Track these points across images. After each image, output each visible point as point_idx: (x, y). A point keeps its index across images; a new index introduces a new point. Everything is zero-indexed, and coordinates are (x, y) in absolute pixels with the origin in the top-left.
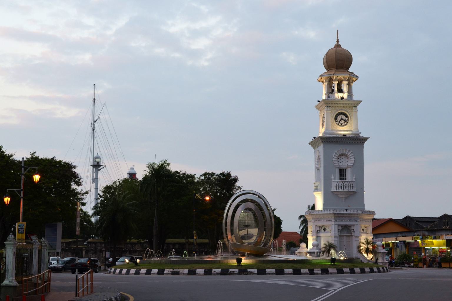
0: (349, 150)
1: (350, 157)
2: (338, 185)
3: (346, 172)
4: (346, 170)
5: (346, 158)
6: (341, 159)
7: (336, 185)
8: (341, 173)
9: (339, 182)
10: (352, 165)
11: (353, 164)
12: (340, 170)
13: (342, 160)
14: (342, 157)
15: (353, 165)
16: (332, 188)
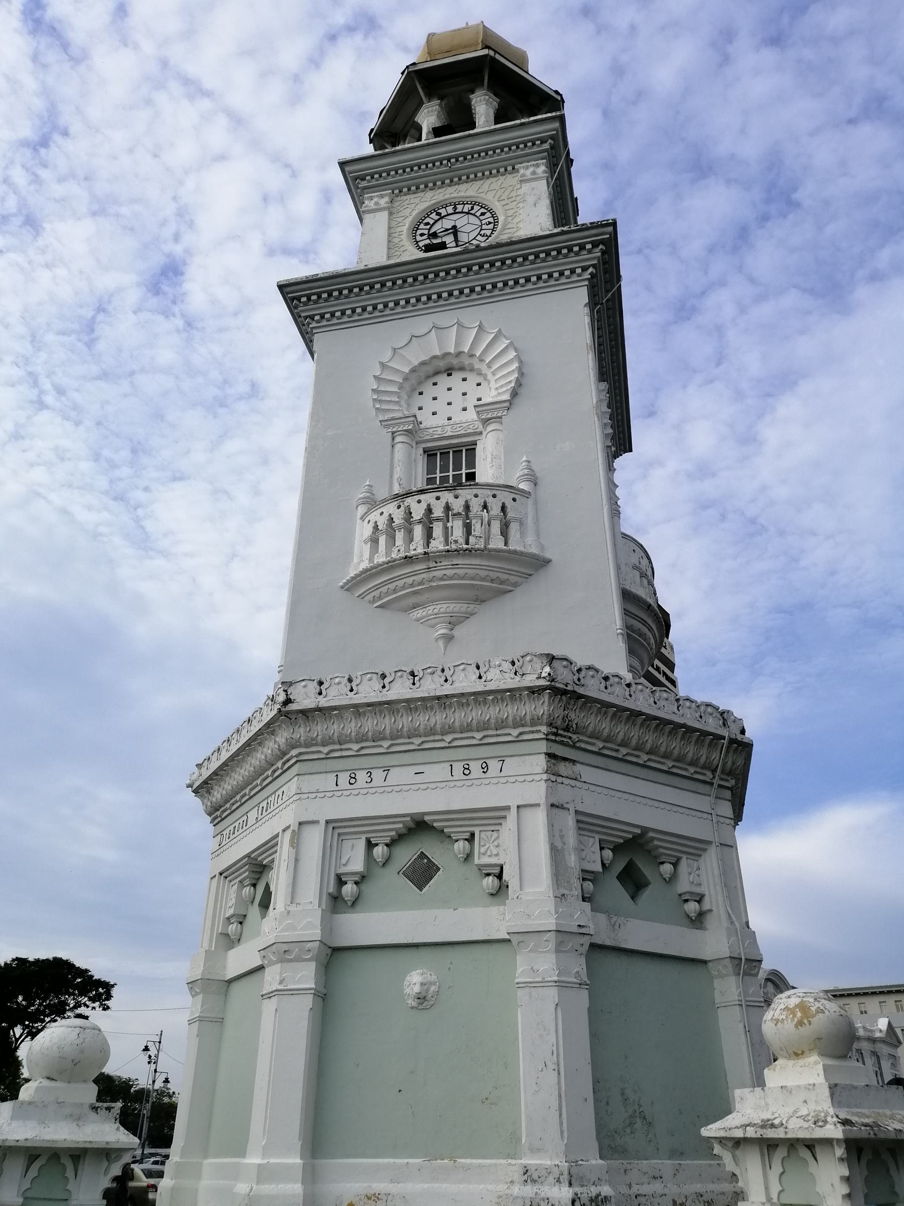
0: (480, 327)
1: (489, 366)
2: (382, 522)
3: (471, 463)
4: (471, 452)
5: (473, 379)
6: (440, 391)
7: (376, 527)
8: (438, 475)
9: (391, 509)
10: (507, 397)
11: (515, 394)
12: (430, 454)
13: (444, 397)
14: (444, 381)
15: (510, 404)
16: (355, 560)
